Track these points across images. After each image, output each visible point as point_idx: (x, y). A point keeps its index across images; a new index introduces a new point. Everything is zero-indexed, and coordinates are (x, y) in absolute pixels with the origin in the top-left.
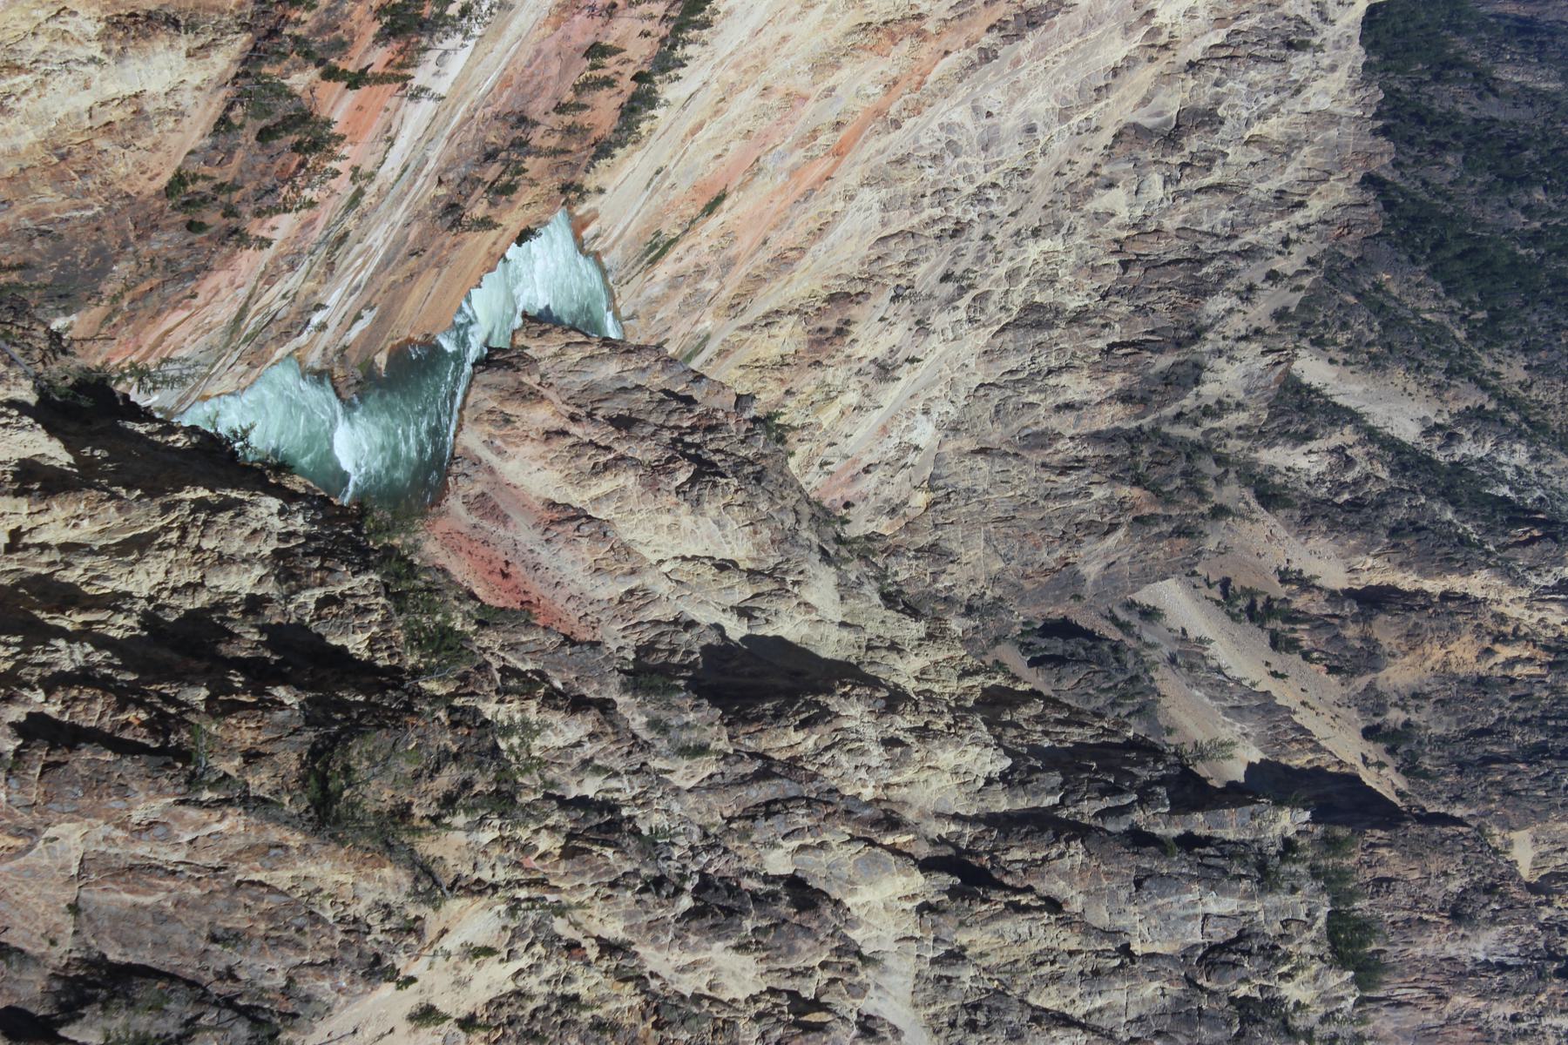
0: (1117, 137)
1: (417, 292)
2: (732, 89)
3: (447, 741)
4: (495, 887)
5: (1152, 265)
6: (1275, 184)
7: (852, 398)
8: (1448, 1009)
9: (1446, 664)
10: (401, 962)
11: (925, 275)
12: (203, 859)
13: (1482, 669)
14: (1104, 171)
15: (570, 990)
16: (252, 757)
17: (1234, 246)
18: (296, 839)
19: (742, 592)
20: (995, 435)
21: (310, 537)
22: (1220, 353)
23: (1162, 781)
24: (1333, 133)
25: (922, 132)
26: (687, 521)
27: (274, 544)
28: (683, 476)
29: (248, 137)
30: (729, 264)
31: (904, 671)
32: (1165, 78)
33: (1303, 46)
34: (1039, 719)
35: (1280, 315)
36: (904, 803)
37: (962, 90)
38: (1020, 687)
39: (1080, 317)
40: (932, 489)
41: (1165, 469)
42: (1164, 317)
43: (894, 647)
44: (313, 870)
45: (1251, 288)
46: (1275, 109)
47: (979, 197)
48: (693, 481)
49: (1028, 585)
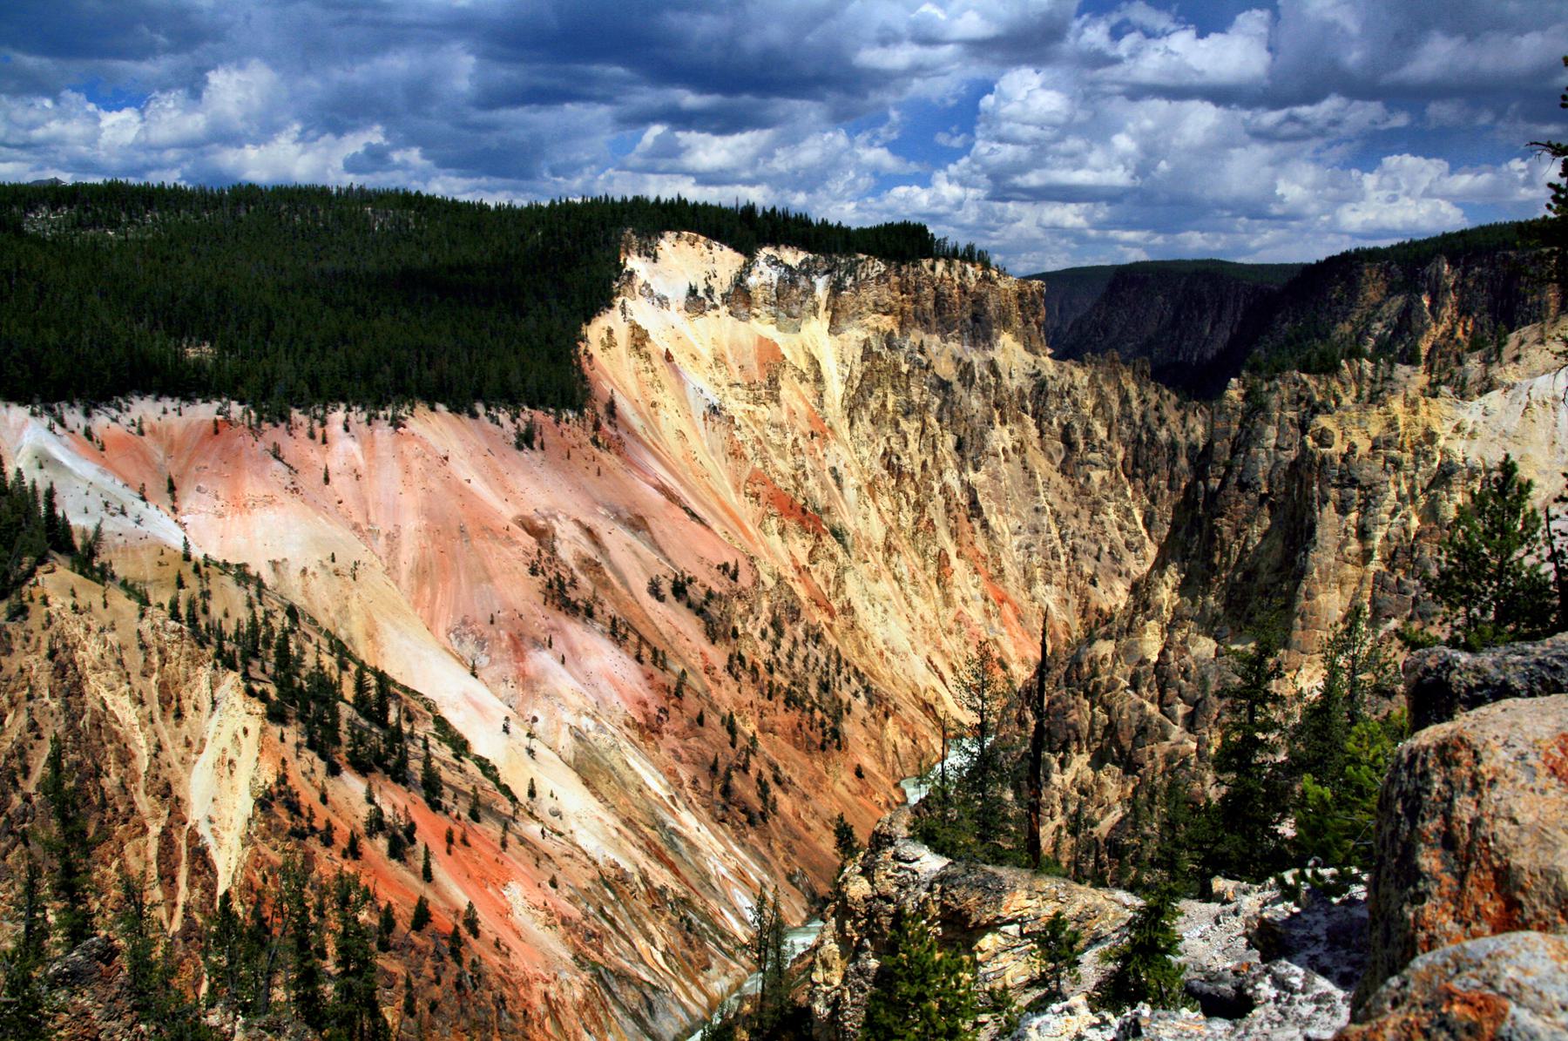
42: (1162, 459)
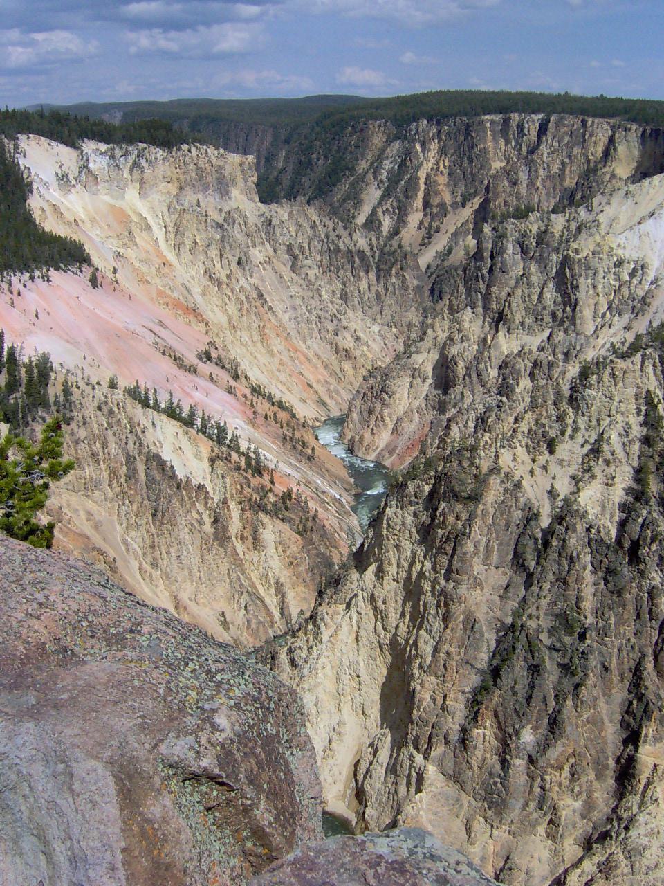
0: (294, 272)
1: (332, 469)
2: (278, 380)
3: (455, 464)
4: (497, 452)
5: (330, 264)
6: (308, 229)
7: (365, 348)
8: (541, 187)
9: (444, 184)
10: (516, 479)
11: (330, 326)
12: (485, 532)
13: (446, 174)
14: (303, 276)
15: (526, 431)
16: (458, 518)
17: (325, 240)
18: (481, 507)
19: (419, 380)
20: (377, 309)
21: (397, 500)
22: (355, 245)
23: (475, 263)
24: (294, 212)
25: (291, 326)
26: (398, 395)
27: (399, 510)
28: (385, 396)
29: (287, 514)
30: (327, 382)
31: (442, 336)
32: (278, 258)
33: (270, 220)
34: (456, 298)
35: (345, 228)
36: (479, 337)
37: (280, 314)
38: (448, 303)
39: (344, 284)
40: (391, 327)
41: (388, 261)
43: (435, 338)
44: (490, 502)
45: (337, 236)
46: (288, 229)
47: (310, 311)
48: (387, 394)
49: (419, 300)
